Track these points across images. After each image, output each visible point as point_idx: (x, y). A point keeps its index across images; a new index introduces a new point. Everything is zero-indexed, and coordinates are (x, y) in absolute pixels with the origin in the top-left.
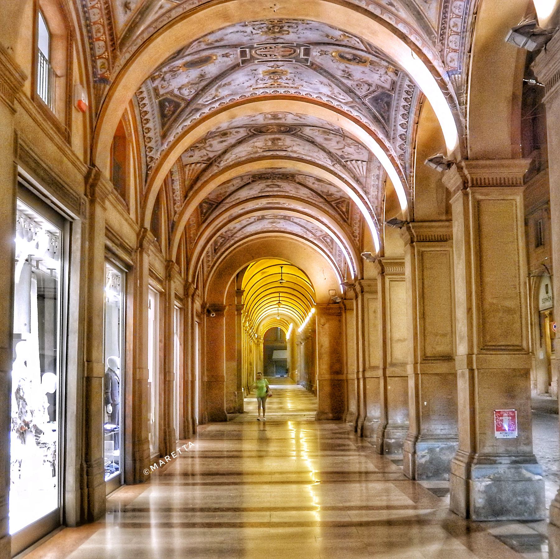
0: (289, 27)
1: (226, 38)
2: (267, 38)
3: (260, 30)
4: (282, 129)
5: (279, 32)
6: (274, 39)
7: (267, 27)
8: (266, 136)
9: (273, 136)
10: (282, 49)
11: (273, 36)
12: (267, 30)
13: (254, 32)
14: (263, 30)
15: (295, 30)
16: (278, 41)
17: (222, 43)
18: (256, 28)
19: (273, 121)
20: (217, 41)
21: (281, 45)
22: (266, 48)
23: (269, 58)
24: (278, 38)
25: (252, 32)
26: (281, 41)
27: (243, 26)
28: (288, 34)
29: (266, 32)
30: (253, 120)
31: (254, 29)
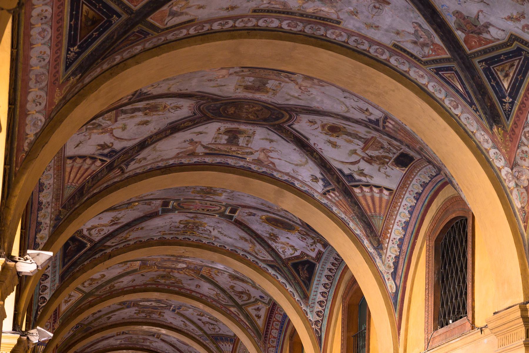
0: (178, 227)
1: (238, 238)
2: (202, 220)
3: (205, 229)
4: (231, 110)
5: (189, 223)
6: (196, 217)
7: (199, 229)
8: (270, 100)
9: (258, 96)
10: (192, 207)
11: (197, 220)
12: (200, 227)
13: (211, 229)
14: (203, 228)
15: (173, 224)
16: (192, 215)
17: (243, 234)
18: (209, 232)
19: (242, 127)
20: (246, 240)
21: (191, 211)
22: (208, 210)
23: (209, 203)
24: (193, 218)
25: (214, 229)
26: (189, 215)
27: (218, 238)
28: (181, 221)
29: (201, 225)
30: (271, 141)
31: (211, 232)
